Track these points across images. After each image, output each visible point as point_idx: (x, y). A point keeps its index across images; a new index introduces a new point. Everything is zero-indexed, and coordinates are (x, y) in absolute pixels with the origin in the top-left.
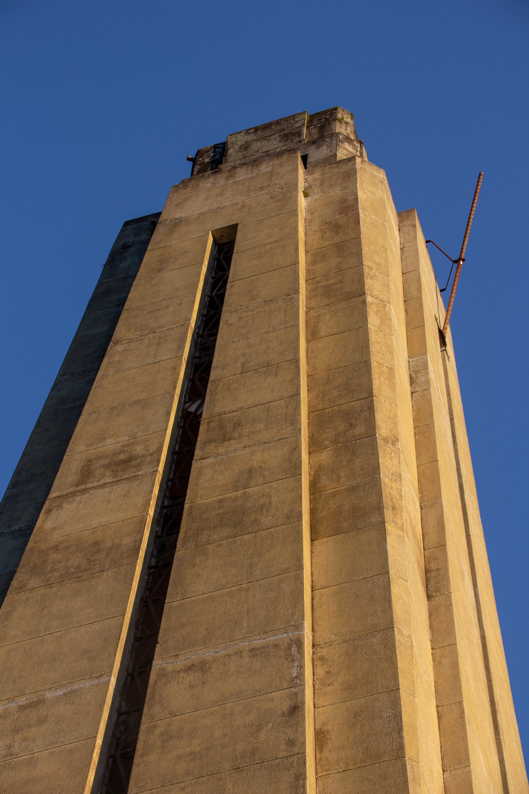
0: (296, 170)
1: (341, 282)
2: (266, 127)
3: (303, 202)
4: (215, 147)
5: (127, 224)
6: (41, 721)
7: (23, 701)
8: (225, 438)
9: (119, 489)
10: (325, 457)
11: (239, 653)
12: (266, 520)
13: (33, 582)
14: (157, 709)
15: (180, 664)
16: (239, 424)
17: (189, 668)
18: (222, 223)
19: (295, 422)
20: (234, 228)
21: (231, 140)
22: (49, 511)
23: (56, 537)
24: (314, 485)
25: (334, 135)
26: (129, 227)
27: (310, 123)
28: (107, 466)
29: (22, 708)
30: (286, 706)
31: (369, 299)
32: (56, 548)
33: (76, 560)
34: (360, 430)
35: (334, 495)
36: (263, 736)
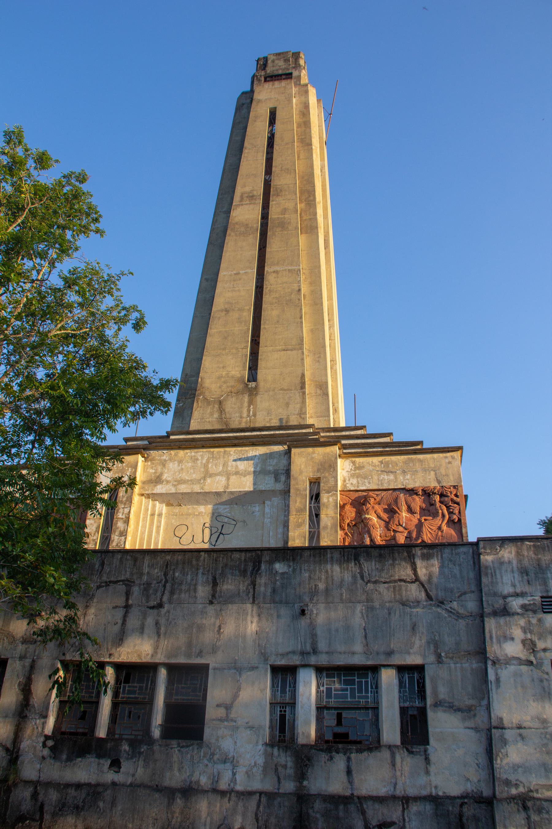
0: (292, 88)
1: (305, 138)
2: (279, 54)
3: (294, 100)
4: (264, 58)
5: (243, 93)
6: (240, 279)
7: (235, 272)
8: (278, 195)
9: (252, 206)
10: (303, 205)
11: (286, 270)
12: (290, 228)
13: (232, 234)
14: (267, 282)
15: (272, 270)
16: (281, 191)
17: (274, 272)
18: (272, 106)
19: (296, 194)
20: (275, 108)
21: (269, 57)
22: (234, 210)
23: (236, 220)
24: (300, 214)
25: (300, 66)
26: (244, 95)
27: (292, 56)
28: (247, 197)
29: (235, 274)
30: (297, 289)
31: (313, 147)
32: (237, 223)
33: (243, 229)
34: (312, 198)
35: (306, 220)
36: (292, 296)
